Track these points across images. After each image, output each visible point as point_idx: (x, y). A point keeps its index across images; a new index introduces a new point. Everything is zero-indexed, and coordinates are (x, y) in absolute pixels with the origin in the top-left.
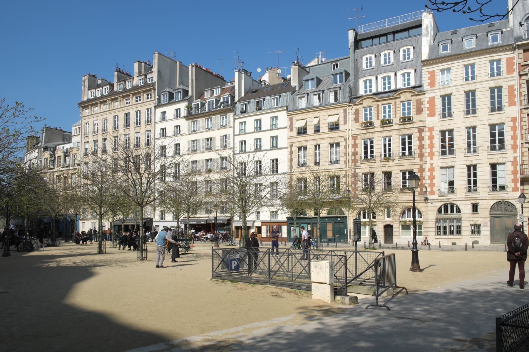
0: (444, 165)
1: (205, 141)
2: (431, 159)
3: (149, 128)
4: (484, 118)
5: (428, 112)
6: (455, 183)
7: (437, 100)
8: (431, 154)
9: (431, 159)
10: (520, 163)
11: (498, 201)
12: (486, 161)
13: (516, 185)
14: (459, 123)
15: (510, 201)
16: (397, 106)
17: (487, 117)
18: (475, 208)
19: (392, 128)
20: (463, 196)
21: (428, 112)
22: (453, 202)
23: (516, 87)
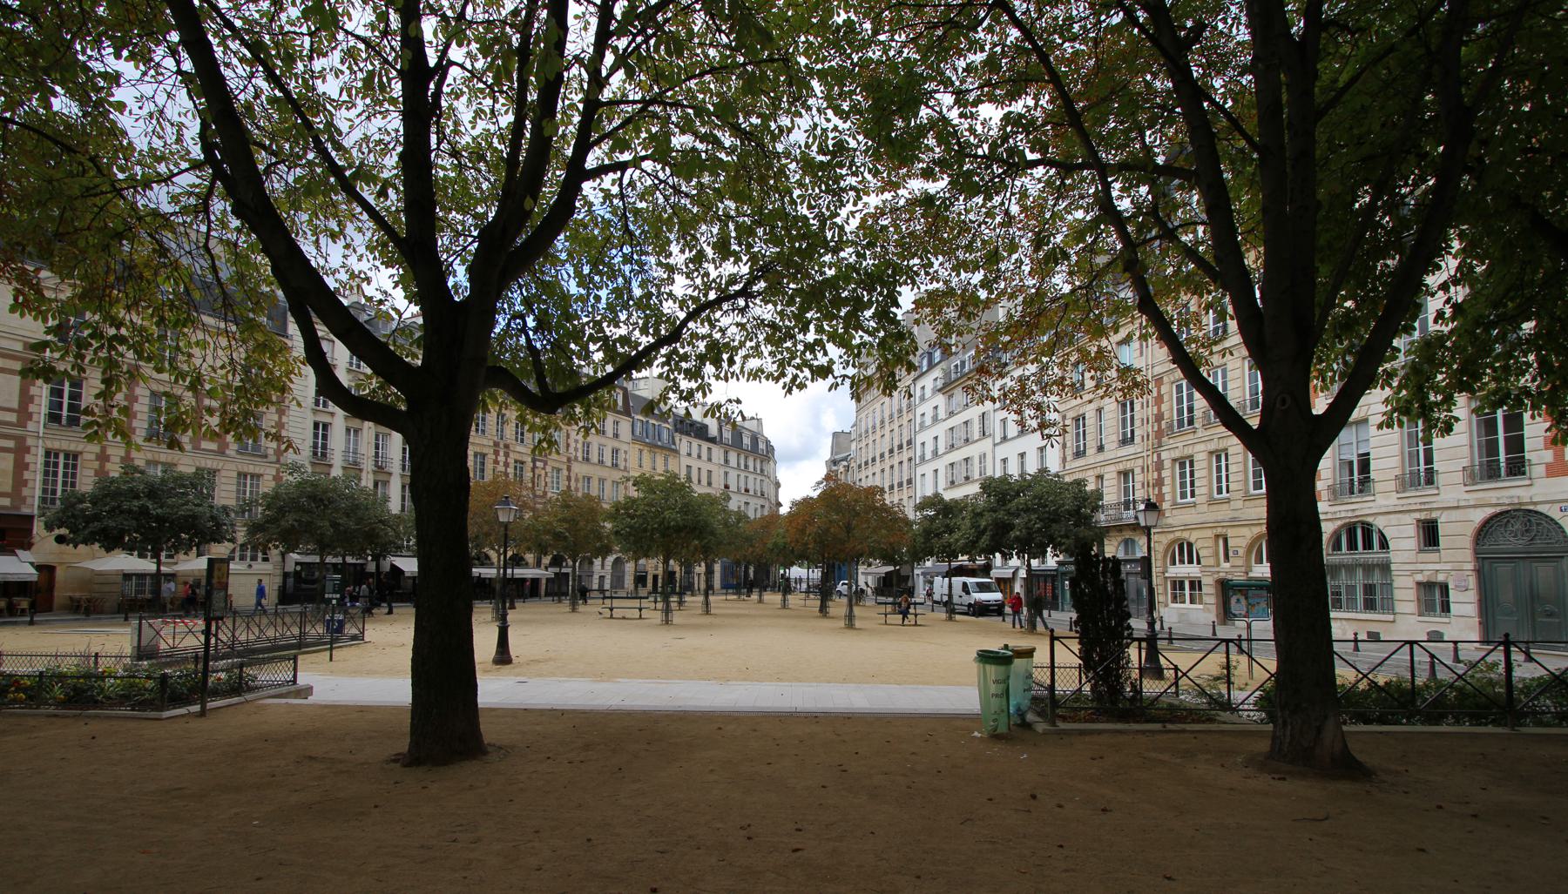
1: (963, 428)
3: (911, 416)
11: (1498, 509)
15: (1540, 508)
18: (1430, 534)
22: (1370, 519)
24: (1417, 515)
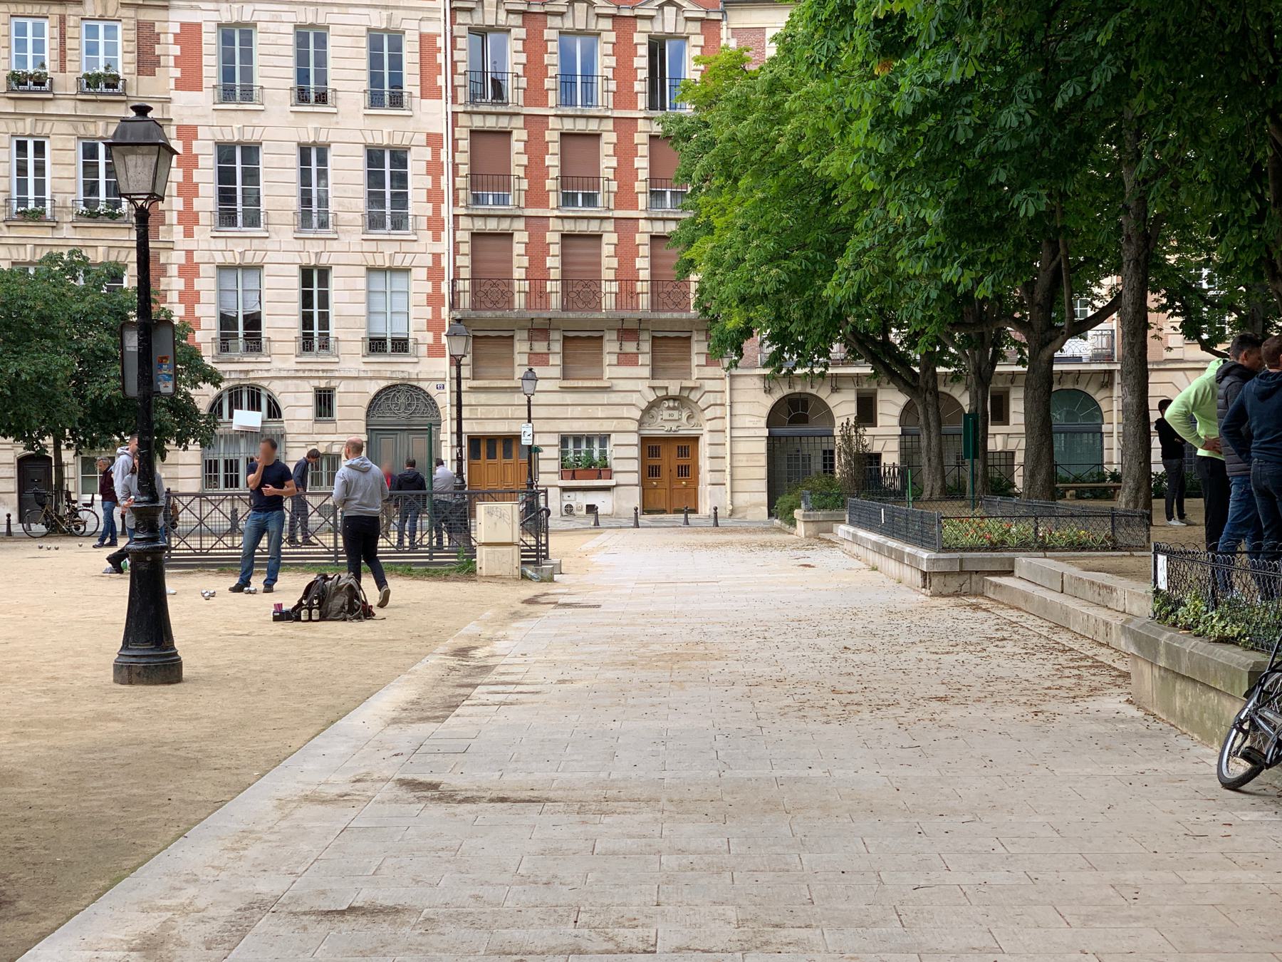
0: (229, 259)
2: (188, 234)
4: (351, 126)
5: (177, 73)
6: (265, 322)
7: (206, 38)
8: (189, 219)
9: (188, 234)
10: (449, 274)
11: (390, 383)
12: (358, 258)
13: (437, 338)
14: (277, 126)
15: (422, 385)
16: (70, 32)
17: (361, 122)
18: (324, 402)
19: (51, 108)
20: (291, 363)
21: (177, 73)
23: (440, 42)
24: (316, 383)
